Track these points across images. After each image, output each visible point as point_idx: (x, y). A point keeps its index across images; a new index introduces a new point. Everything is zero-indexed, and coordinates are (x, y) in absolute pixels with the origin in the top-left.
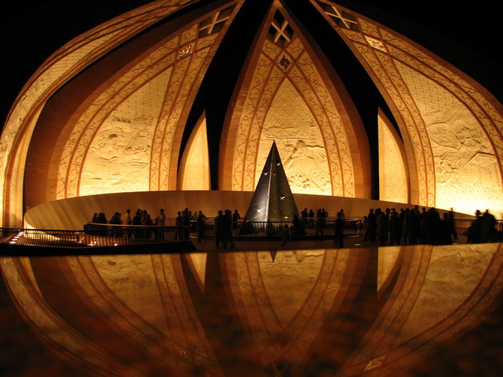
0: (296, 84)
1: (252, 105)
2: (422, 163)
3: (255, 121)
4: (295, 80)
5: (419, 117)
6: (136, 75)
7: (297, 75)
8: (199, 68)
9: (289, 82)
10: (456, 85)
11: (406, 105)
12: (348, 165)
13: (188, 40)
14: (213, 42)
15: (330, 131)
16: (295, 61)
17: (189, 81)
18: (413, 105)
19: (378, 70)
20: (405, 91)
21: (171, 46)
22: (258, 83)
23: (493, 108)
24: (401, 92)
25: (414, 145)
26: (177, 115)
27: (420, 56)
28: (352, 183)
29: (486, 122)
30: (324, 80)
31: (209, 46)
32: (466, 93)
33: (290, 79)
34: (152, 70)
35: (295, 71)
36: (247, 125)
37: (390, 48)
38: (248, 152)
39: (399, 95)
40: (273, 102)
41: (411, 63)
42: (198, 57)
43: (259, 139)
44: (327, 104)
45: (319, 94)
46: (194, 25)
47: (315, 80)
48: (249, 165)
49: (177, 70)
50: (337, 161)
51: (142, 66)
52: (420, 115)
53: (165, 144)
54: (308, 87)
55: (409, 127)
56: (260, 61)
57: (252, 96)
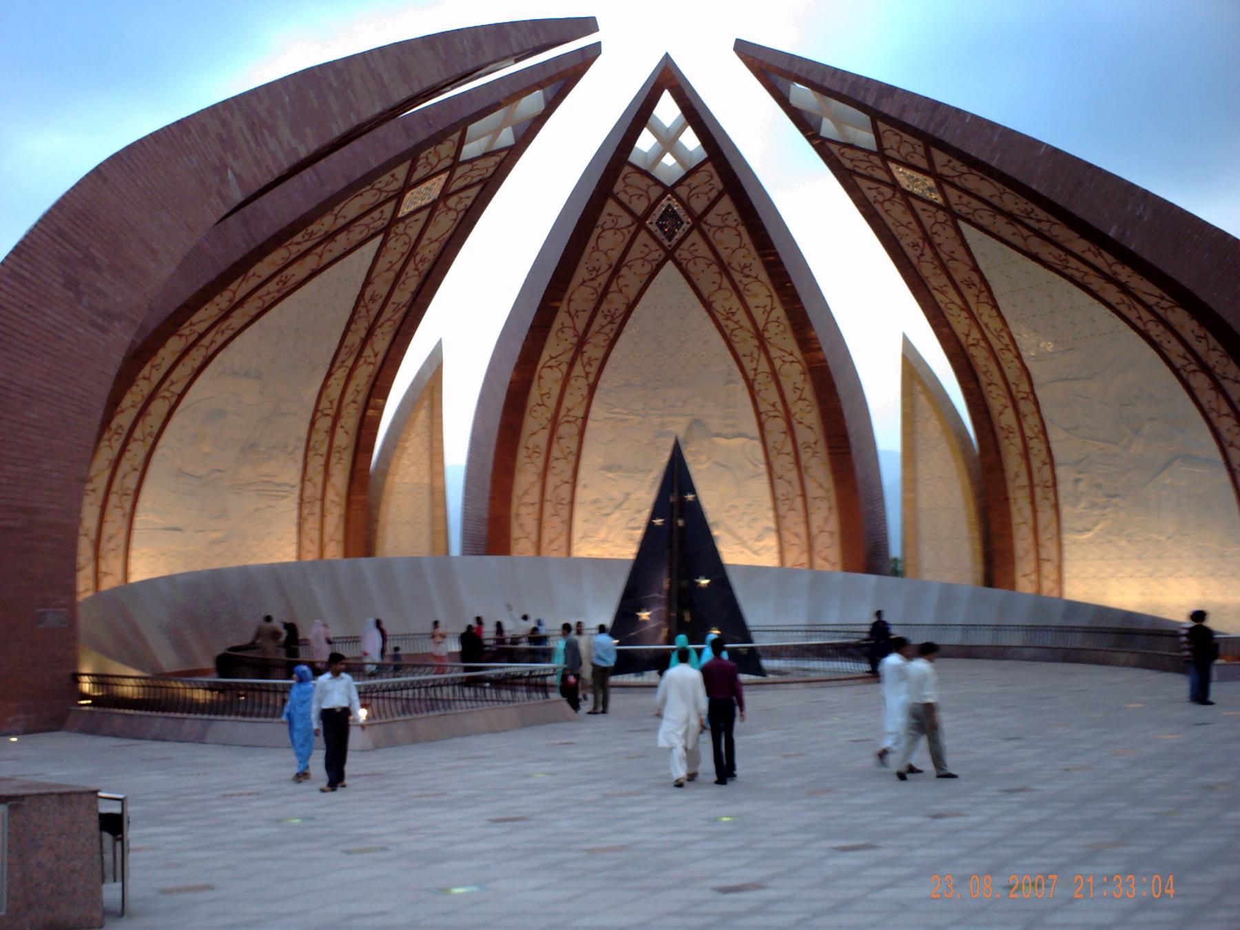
0: (694, 278)
1: (574, 328)
2: (1023, 480)
3: (578, 370)
4: (691, 267)
5: (1016, 361)
6: (293, 257)
7: (699, 253)
8: (447, 235)
9: (676, 271)
10: (1124, 289)
11: (981, 331)
12: (821, 486)
14: (491, 171)
15: (774, 396)
16: (698, 221)
18: (1003, 334)
19: (915, 245)
20: (983, 297)
21: (388, 184)
23: (1220, 347)
24: (972, 301)
25: (1001, 435)
26: (376, 355)
27: (1032, 215)
28: (832, 533)
29: (1200, 382)
31: (480, 181)
32: (1149, 308)
33: (678, 265)
34: (332, 245)
35: (693, 244)
36: (556, 381)
37: (953, 194)
38: (555, 452)
39: (967, 308)
40: (630, 321)
41: (1006, 230)
42: (450, 209)
43: (585, 418)
44: (771, 327)
45: (751, 302)
47: (745, 267)
48: (556, 487)
49: (391, 243)
50: (793, 475)
51: (312, 234)
52: (1019, 357)
53: (339, 431)
54: (726, 283)
55: (990, 388)
56: (603, 218)
57: (573, 306)
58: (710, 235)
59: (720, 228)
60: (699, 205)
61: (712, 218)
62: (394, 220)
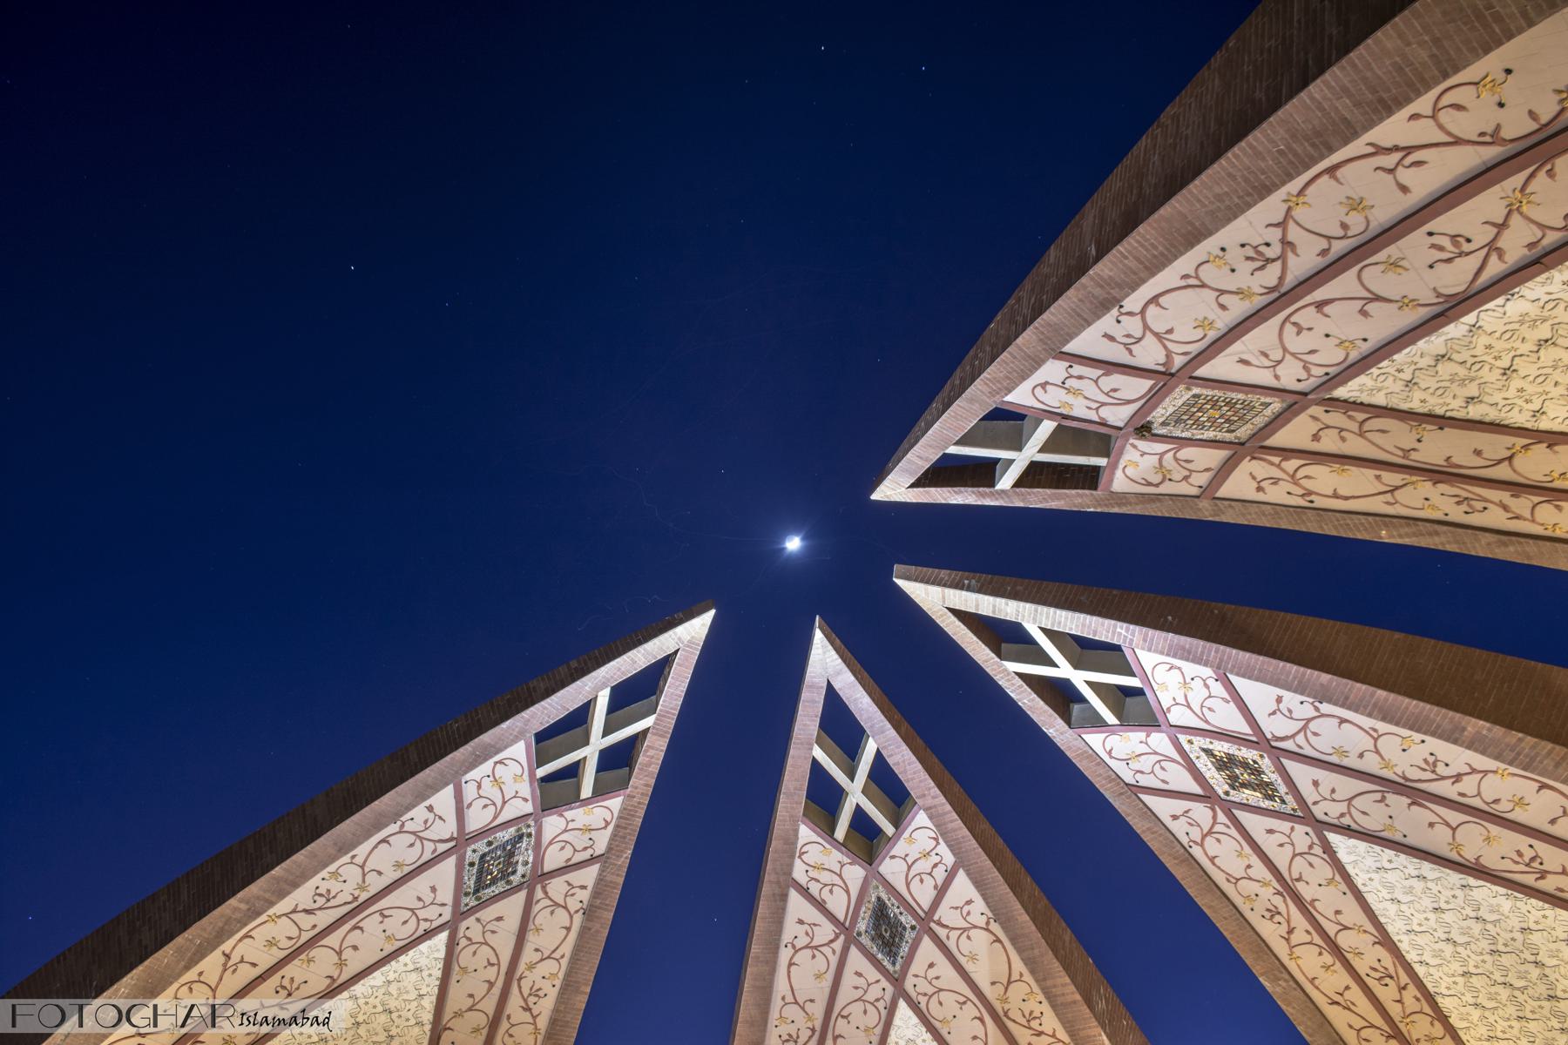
0: (1398, 837)
1: (1372, 1026)
4: (1370, 824)
9: (1362, 846)
13: (847, 891)
17: (1040, 1034)
22: (1277, 918)
30: (1452, 736)
33: (1347, 831)
35: (1316, 783)
40: (1420, 971)
42: (965, 930)
46: (796, 831)
49: (934, 1009)
54: (1454, 817)
56: (1179, 828)
58: (1308, 751)
59: (1304, 728)
60: (1228, 718)
61: (1274, 727)
62: (897, 981)
